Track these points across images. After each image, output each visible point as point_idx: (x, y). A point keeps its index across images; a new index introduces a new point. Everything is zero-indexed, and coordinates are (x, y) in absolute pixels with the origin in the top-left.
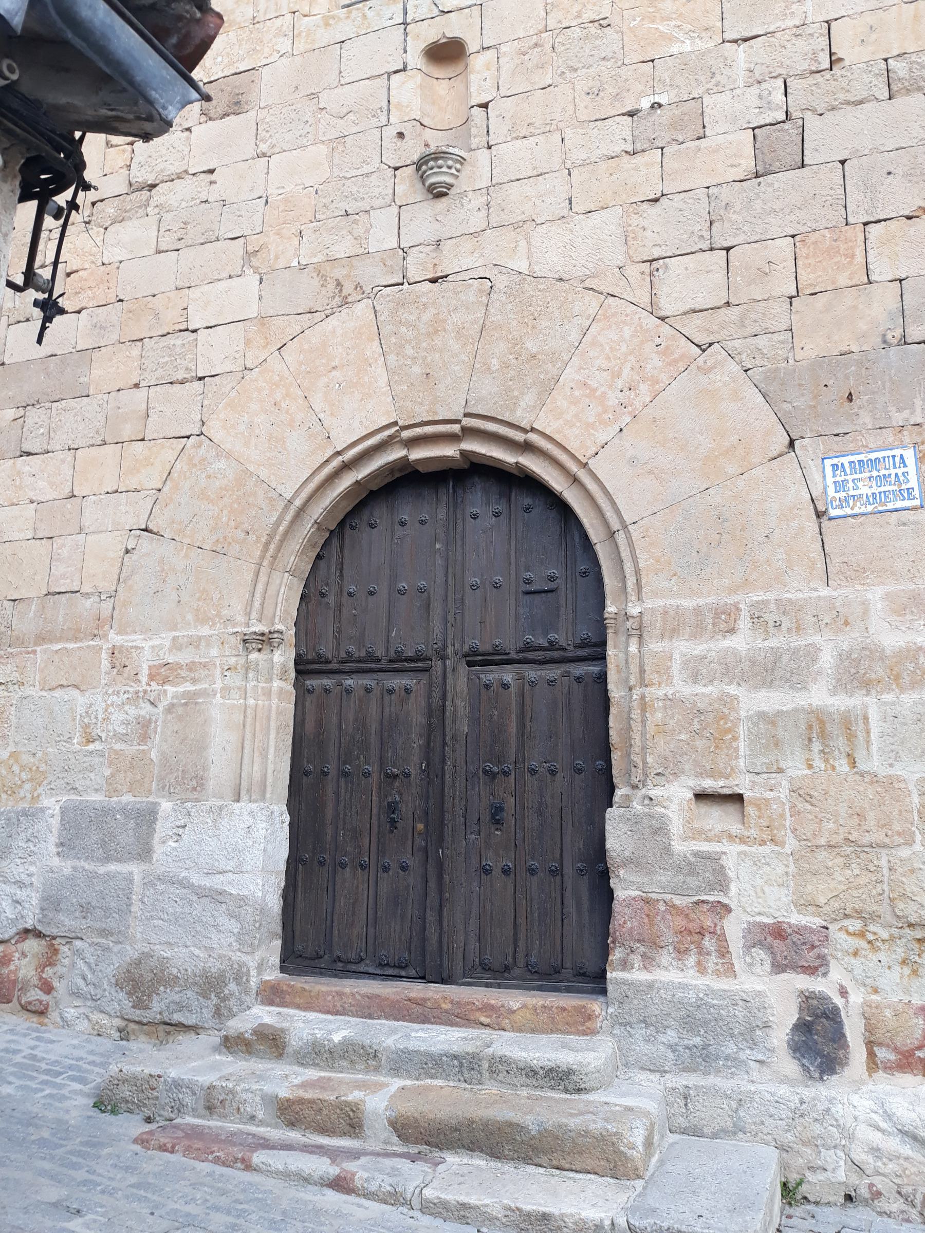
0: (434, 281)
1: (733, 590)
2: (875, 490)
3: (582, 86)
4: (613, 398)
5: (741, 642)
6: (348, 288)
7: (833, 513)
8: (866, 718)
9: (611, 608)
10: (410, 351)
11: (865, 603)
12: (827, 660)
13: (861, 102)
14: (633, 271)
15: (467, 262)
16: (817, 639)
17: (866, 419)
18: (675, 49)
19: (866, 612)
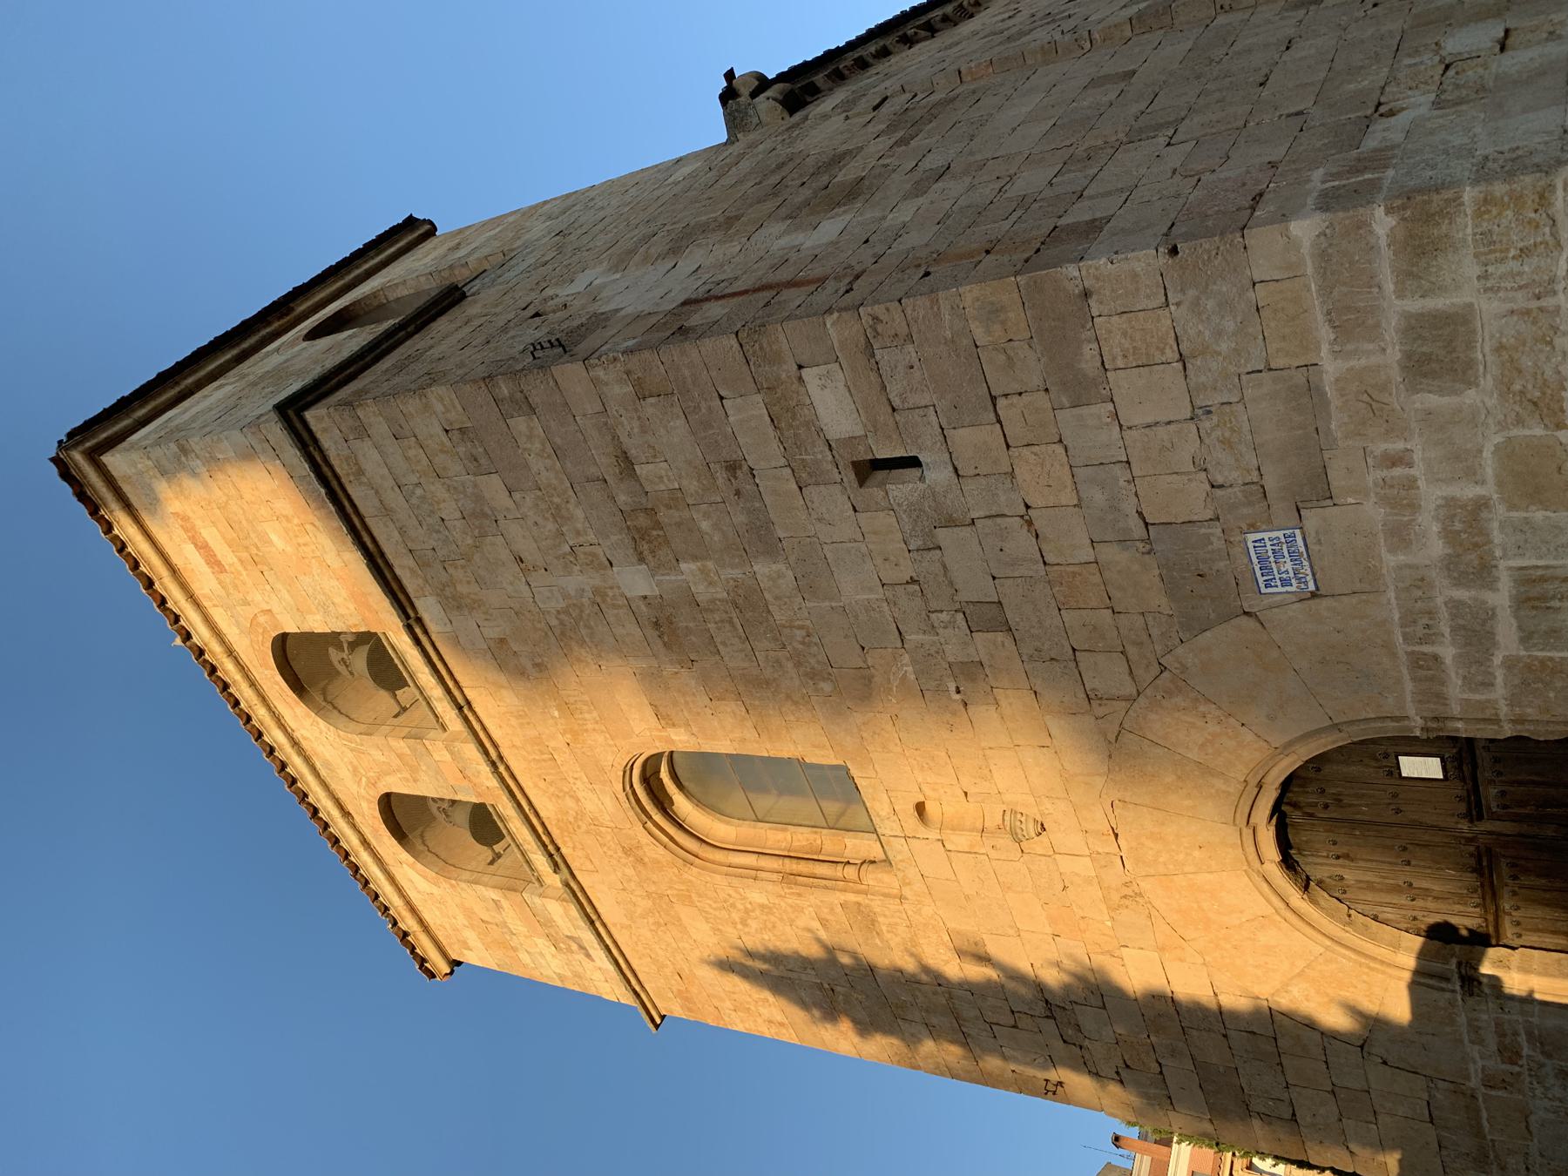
0: (1116, 836)
1: (1394, 655)
2: (1288, 559)
6: (1128, 891)
7: (1312, 587)
8: (1522, 568)
9: (1418, 733)
10: (1181, 857)
11: (1400, 568)
12: (1462, 594)
13: (945, 567)
14: (1100, 711)
16: (1440, 601)
17: (1221, 565)
19: (1410, 566)
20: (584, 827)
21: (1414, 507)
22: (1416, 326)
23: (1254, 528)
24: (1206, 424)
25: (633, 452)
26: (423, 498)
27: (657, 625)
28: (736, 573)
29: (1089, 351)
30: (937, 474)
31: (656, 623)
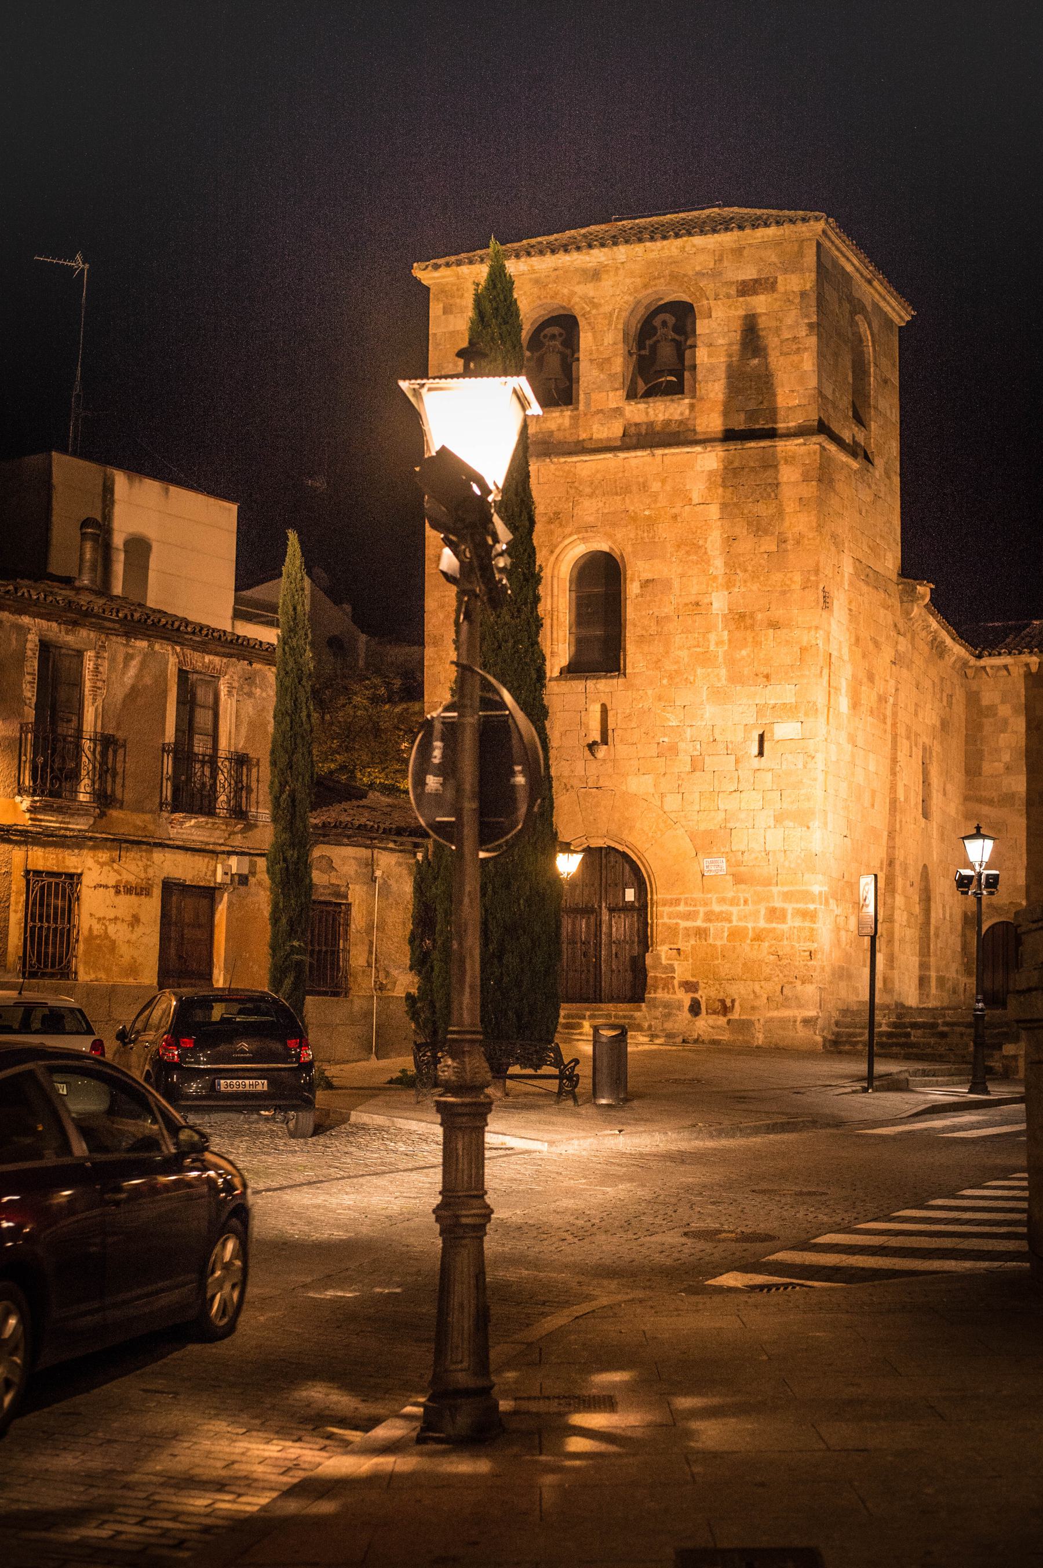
3: (642, 730)
4: (650, 834)
5: (681, 908)
6: (569, 786)
12: (701, 915)
15: (607, 784)
18: (671, 724)
20: (572, 491)
21: (731, 905)
22: (784, 911)
23: (728, 861)
24: (763, 854)
25: (778, 632)
26: (770, 496)
27: (697, 604)
28: (720, 659)
29: (791, 824)
30: (756, 763)
31: (697, 604)
